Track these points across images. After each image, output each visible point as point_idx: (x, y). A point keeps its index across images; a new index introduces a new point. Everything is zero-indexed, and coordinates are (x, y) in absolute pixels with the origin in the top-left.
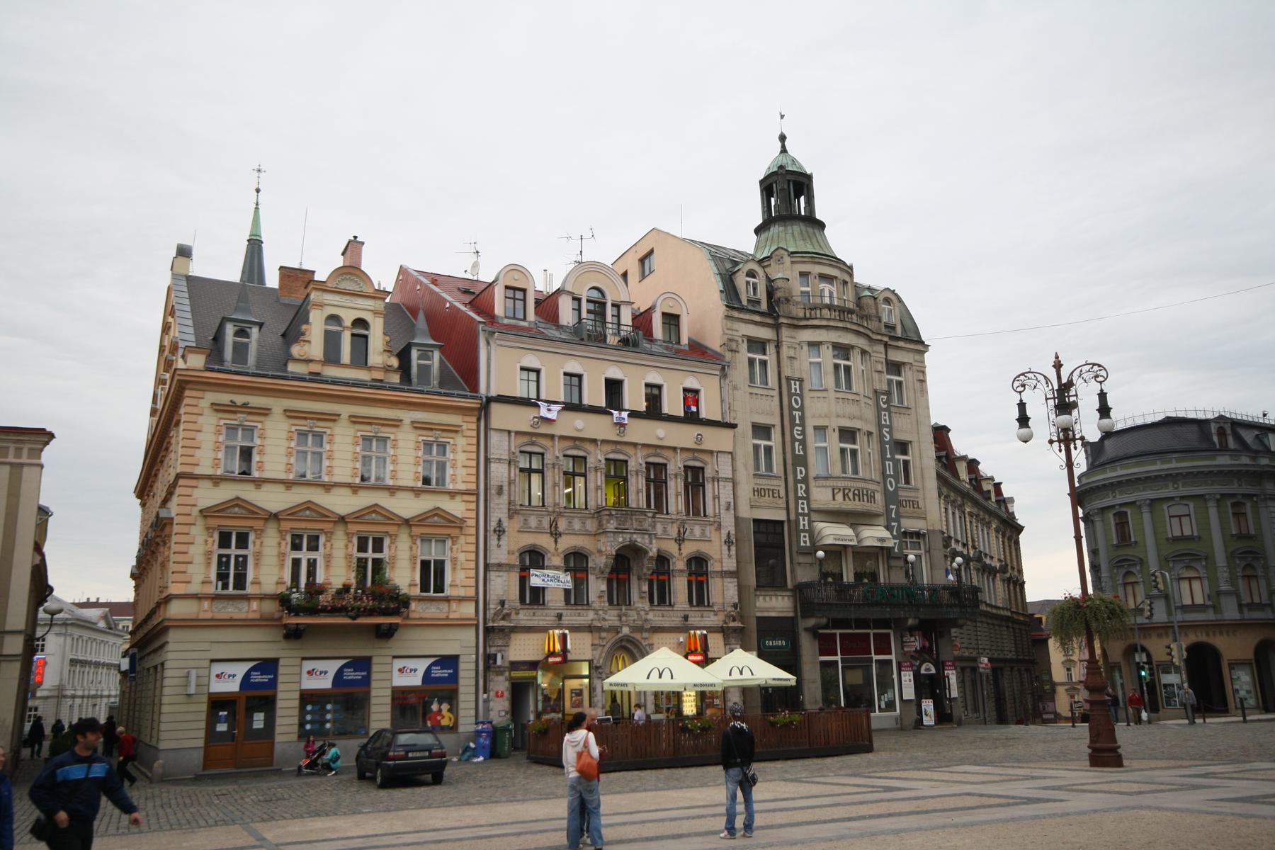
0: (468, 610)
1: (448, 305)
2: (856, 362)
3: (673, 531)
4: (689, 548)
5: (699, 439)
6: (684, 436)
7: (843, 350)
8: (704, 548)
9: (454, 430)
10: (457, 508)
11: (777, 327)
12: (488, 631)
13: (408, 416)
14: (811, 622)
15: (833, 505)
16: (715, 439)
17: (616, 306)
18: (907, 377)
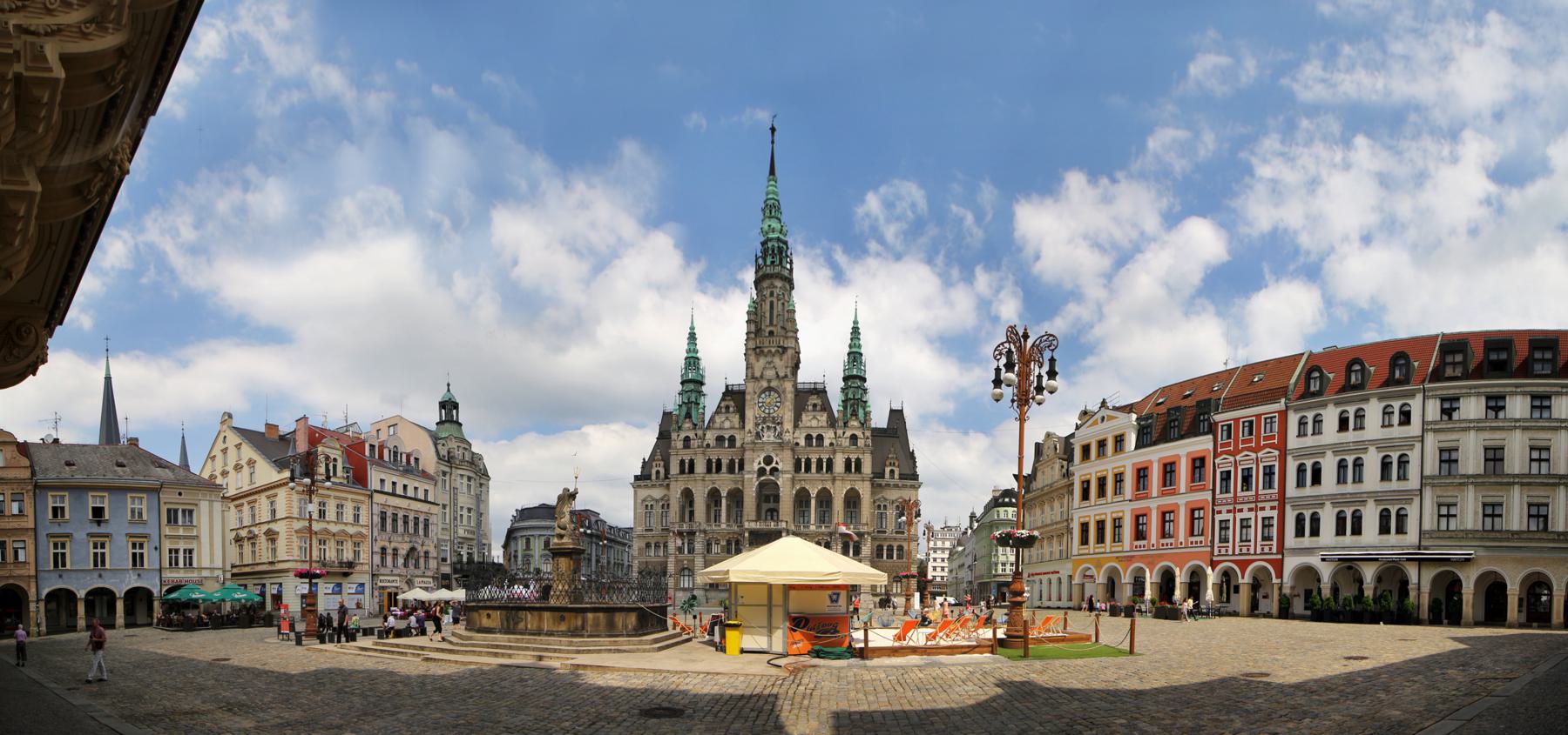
0: (366, 568)
1: (317, 435)
2: (472, 483)
3: (420, 542)
4: (425, 548)
5: (409, 505)
6: (404, 503)
7: (469, 479)
8: (429, 548)
9: (362, 502)
10: (364, 531)
11: (451, 467)
12: (373, 575)
13: (350, 496)
14: (457, 576)
15: (464, 536)
16: (435, 509)
17: (401, 454)
18: (484, 489)
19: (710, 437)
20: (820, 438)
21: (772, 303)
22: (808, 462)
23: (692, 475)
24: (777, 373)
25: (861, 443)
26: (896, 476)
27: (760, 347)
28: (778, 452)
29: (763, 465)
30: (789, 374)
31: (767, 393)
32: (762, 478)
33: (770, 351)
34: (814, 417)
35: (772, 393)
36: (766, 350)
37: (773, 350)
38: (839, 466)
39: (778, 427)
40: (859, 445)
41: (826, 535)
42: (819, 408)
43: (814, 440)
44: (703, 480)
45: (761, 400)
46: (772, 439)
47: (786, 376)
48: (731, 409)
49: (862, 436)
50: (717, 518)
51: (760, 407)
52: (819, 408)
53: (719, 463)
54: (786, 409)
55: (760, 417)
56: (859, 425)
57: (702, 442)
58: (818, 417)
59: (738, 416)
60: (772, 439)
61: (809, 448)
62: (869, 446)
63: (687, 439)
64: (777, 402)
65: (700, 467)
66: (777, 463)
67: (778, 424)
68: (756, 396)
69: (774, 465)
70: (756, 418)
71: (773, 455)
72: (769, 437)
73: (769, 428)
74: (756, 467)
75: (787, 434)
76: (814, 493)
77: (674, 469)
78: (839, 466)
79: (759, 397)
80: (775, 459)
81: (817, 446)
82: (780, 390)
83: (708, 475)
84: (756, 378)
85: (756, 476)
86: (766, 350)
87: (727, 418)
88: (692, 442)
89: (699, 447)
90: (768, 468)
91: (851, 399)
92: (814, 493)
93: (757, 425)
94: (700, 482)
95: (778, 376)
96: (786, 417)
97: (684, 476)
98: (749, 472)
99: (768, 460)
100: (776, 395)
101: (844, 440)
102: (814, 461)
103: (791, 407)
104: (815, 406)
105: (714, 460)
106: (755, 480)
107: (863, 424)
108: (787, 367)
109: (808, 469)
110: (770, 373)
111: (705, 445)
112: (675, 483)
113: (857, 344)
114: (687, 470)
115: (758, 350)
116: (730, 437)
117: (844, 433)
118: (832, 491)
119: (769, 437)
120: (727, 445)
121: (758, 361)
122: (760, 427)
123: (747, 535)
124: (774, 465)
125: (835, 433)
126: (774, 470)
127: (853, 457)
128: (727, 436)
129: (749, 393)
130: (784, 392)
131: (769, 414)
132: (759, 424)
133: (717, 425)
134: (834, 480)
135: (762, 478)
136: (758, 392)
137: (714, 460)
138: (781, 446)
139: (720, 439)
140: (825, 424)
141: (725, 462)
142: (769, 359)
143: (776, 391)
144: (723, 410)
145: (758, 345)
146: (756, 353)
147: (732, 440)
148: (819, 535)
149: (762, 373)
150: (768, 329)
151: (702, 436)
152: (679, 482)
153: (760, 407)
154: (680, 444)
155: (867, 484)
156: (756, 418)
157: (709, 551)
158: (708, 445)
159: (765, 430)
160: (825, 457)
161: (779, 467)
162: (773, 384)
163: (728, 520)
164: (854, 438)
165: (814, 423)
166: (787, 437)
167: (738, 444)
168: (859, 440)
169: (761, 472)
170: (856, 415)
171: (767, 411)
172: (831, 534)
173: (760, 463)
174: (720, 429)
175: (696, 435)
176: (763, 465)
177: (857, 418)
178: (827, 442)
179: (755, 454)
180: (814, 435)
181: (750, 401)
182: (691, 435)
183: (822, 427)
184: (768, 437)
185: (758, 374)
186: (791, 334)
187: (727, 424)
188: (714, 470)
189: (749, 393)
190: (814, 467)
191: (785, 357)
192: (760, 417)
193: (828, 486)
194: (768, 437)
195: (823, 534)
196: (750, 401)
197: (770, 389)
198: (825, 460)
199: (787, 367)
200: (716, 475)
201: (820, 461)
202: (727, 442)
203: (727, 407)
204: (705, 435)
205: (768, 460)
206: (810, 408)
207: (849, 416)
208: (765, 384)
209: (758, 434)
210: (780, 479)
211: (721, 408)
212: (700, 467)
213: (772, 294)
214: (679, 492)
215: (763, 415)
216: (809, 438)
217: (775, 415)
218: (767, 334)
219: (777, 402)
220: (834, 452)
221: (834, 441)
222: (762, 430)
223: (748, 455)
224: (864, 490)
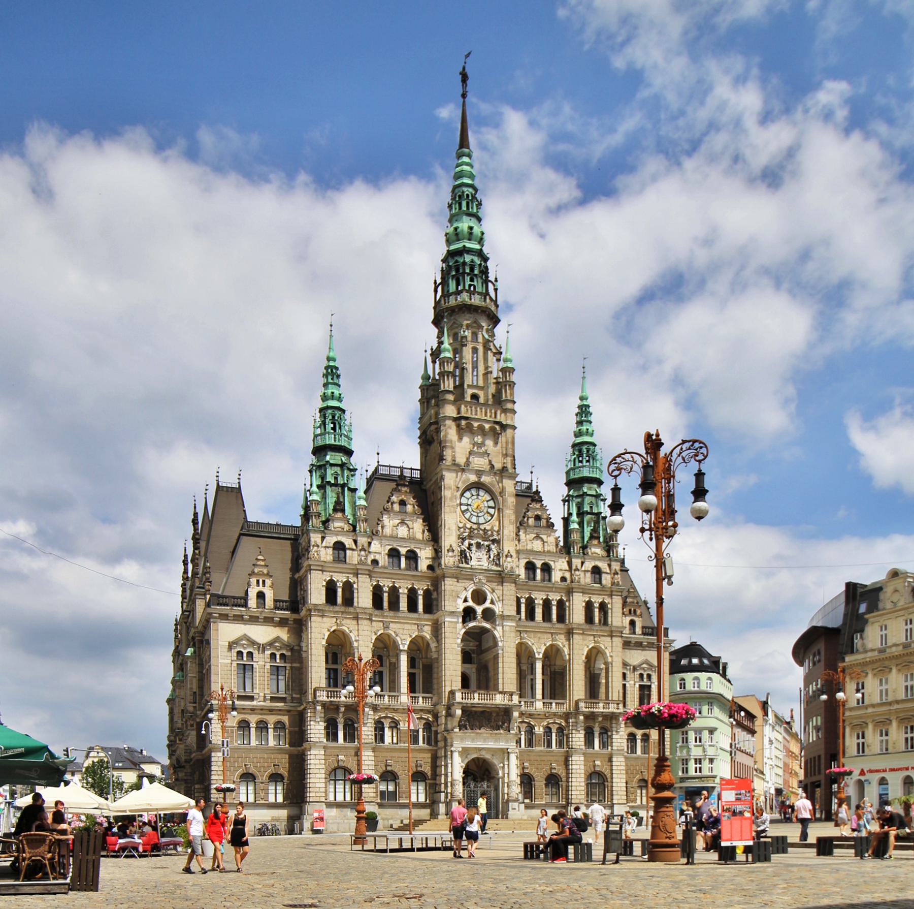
19: (380, 550)
20: (547, 568)
21: (475, 350)
22: (530, 603)
23: (351, 609)
24: (490, 461)
25: (606, 579)
26: (638, 630)
27: (466, 418)
28: (494, 585)
29: (470, 603)
30: (509, 466)
31: (474, 492)
32: (472, 624)
33: (481, 428)
34: (538, 537)
35: (482, 493)
36: (476, 424)
37: (487, 426)
38: (577, 615)
39: (493, 547)
40: (604, 582)
41: (560, 717)
42: (543, 522)
43: (538, 572)
44: (370, 620)
45: (464, 501)
46: (485, 564)
47: (504, 469)
48: (409, 508)
49: (608, 571)
50: (394, 686)
51: (463, 512)
52: (543, 522)
53: (394, 591)
54: (506, 522)
55: (465, 527)
56: (604, 554)
58: (544, 537)
59: (420, 521)
60: (485, 564)
61: (531, 583)
62: (618, 582)
63: (339, 547)
64: (489, 507)
65: (364, 599)
66: (492, 602)
67: (494, 541)
68: (459, 494)
69: (487, 604)
71: (487, 589)
72: (479, 560)
73: (479, 546)
74: (461, 606)
75: (509, 559)
76: (539, 651)
77: (316, 595)
78: (577, 615)
79: (462, 495)
80: (489, 597)
81: (543, 580)
82: (496, 489)
83: (377, 612)
84: (458, 465)
85: (461, 620)
86: (476, 424)
87: (403, 522)
88: (348, 552)
89: (361, 563)
90: (479, 609)
91: (588, 513)
92: (539, 651)
94: (366, 622)
95: (492, 467)
96: (506, 532)
97: (337, 609)
98: (452, 613)
99: (479, 596)
100: (489, 498)
101: (582, 574)
102: (539, 602)
103: (513, 518)
104: (538, 518)
105: (386, 589)
106: (460, 625)
107: (608, 551)
108: (506, 455)
109: (531, 615)
110: (479, 462)
111: (369, 562)
112: (319, 619)
113: (590, 430)
114: (339, 600)
115: (463, 423)
116: (408, 551)
117: (582, 563)
118: (566, 650)
119: (479, 560)
120: (403, 565)
121: (460, 439)
122: (466, 543)
123: (459, 712)
124: (487, 604)
125: (570, 564)
126: (488, 615)
127: (597, 600)
128: (403, 551)
129: (450, 488)
130: (502, 493)
132: (463, 539)
133: (388, 531)
134: (569, 633)
135: (472, 624)
136: (462, 487)
137: (386, 589)
138: (501, 577)
139: (394, 554)
140: (552, 548)
141: (403, 591)
142: (479, 439)
143: (488, 491)
144: (396, 507)
145: (463, 414)
146: (458, 426)
147: (412, 557)
148: (547, 718)
149: (468, 459)
150: (470, 392)
151: (366, 545)
152: (325, 619)
153: (463, 512)
154: (327, 555)
155: (618, 642)
156: (460, 528)
157: (380, 737)
158: (375, 562)
159: (474, 548)
160: (554, 597)
161: (497, 609)
162: (485, 479)
163: (412, 688)
164: (596, 571)
165: (537, 546)
166: (509, 564)
167: (423, 564)
168: (604, 576)
169: (468, 614)
170: (598, 538)
171: (474, 519)
172: (567, 716)
173: (465, 600)
175: (355, 542)
176: (470, 603)
177: (599, 542)
178: (556, 576)
179: (462, 584)
180: (539, 564)
181: (451, 499)
182: (348, 542)
183: (549, 552)
184: (479, 560)
185: (461, 460)
186: (509, 406)
187: (403, 532)
188: (386, 604)
189: (450, 488)
190: (539, 611)
191: (502, 439)
192: (465, 527)
193: (561, 641)
194: (479, 560)
195: (555, 715)
196: (451, 499)
197: (478, 486)
198: (554, 603)
199: (506, 455)
200: (392, 614)
201: (547, 604)
202: (403, 560)
203: (403, 503)
204: (370, 543)
205: (479, 596)
206: (531, 521)
207: (586, 539)
208: (473, 478)
209: (463, 554)
210: (499, 628)
211: (392, 504)
212: (364, 599)
213: (475, 335)
214: (327, 634)
215: (468, 526)
216: (530, 567)
217: (488, 528)
218: (468, 399)
219: (489, 507)
220: (569, 592)
221: (567, 575)
222: (469, 548)
223: (449, 585)
224: (613, 650)
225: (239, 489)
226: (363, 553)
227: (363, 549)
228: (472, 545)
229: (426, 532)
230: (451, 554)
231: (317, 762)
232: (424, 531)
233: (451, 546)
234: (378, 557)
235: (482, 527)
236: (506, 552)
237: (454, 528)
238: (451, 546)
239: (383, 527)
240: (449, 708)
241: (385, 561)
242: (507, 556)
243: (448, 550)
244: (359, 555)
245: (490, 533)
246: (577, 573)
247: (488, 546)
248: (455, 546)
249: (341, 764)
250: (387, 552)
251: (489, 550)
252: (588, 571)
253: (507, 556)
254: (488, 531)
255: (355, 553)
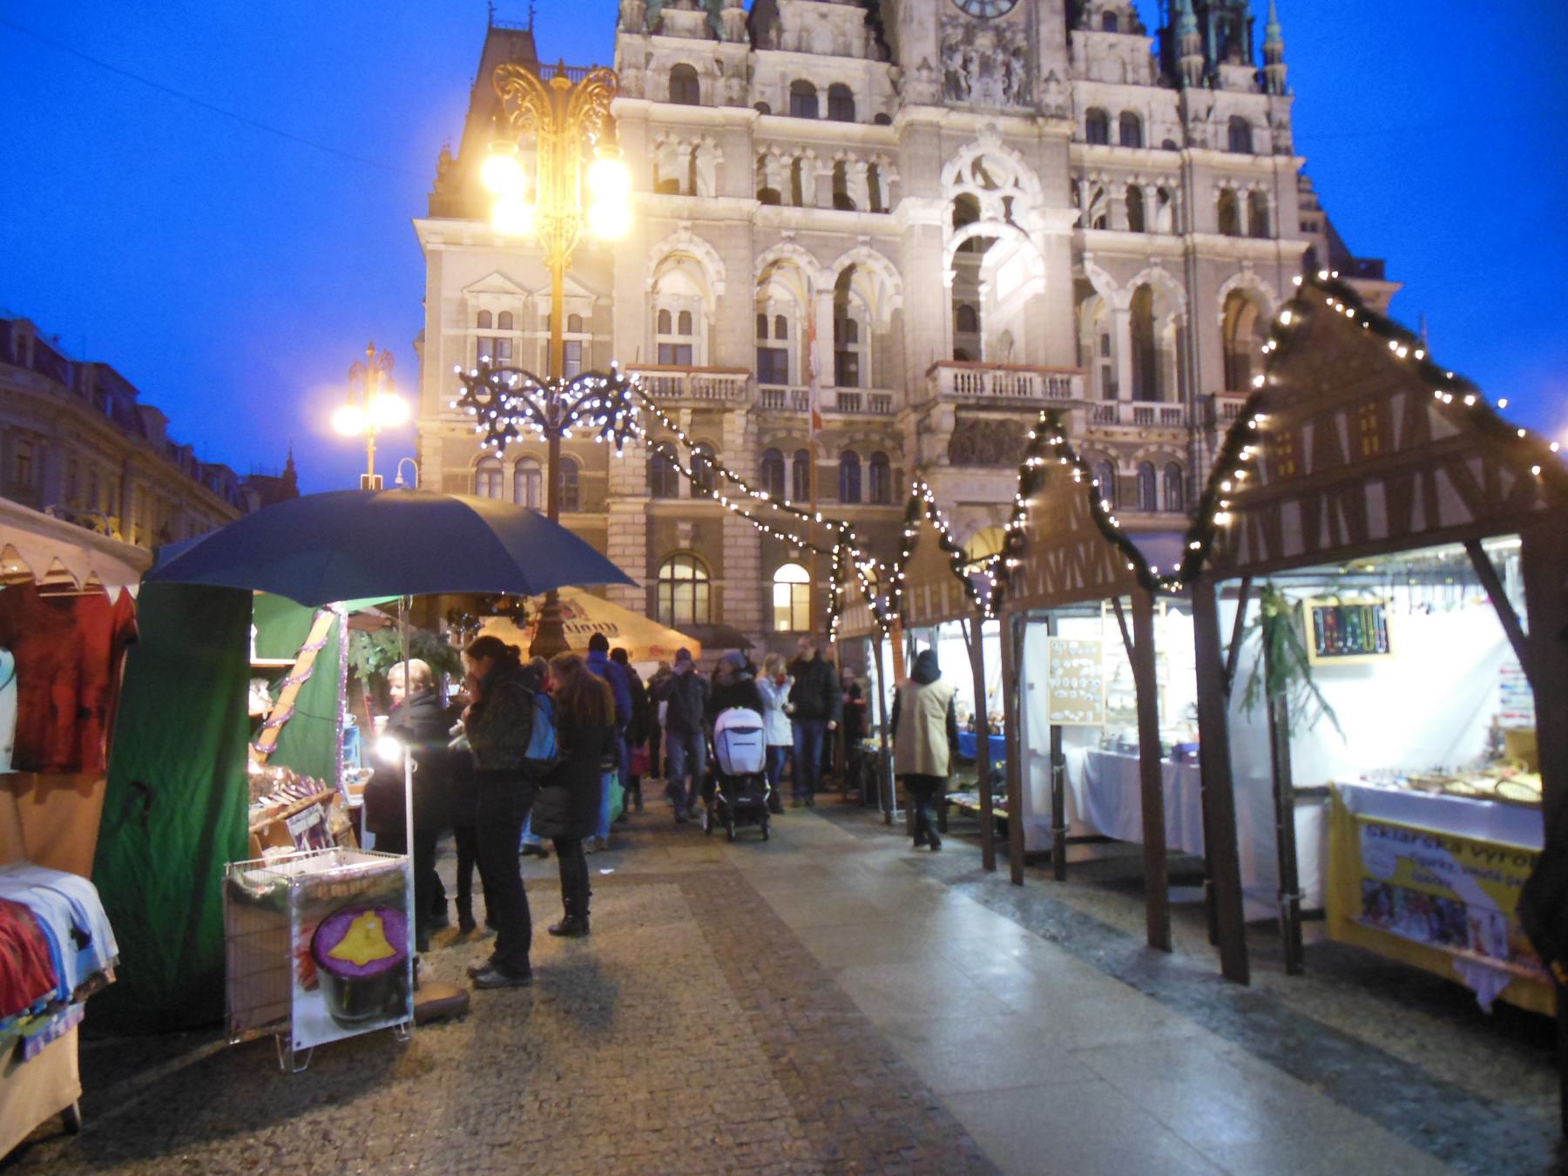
39: (1017, 65)
40: (1257, 146)
57: (745, 90)
67: (1016, 53)
70: (941, 26)
75: (1053, 86)
93: (946, 50)
96: (1044, 30)
131: (982, 17)
133: (789, 38)
159: (974, 67)
173: (959, 179)
174: (798, 50)
178: (1154, 132)
180: (1115, 112)
206: (1096, 20)
215: (963, 18)
225: (528, 36)
226: (735, 82)
227: (736, 75)
228: (971, 60)
229: (872, 42)
230: (925, 73)
231: (629, 539)
232: (867, 39)
233: (925, 60)
234: (769, 91)
235: (992, 22)
236: (1045, 73)
237: (931, 24)
238: (925, 60)
239: (780, 31)
240: (924, 407)
241: (784, 102)
242: (1047, 80)
243: (919, 69)
244: (729, 87)
245: (1008, 35)
246: (1200, 126)
247: (1007, 66)
248: (933, 62)
249: (684, 544)
250: (788, 83)
251: (1009, 73)
252: (1221, 123)
253: (1047, 80)
254: (1004, 30)
255: (721, 82)
